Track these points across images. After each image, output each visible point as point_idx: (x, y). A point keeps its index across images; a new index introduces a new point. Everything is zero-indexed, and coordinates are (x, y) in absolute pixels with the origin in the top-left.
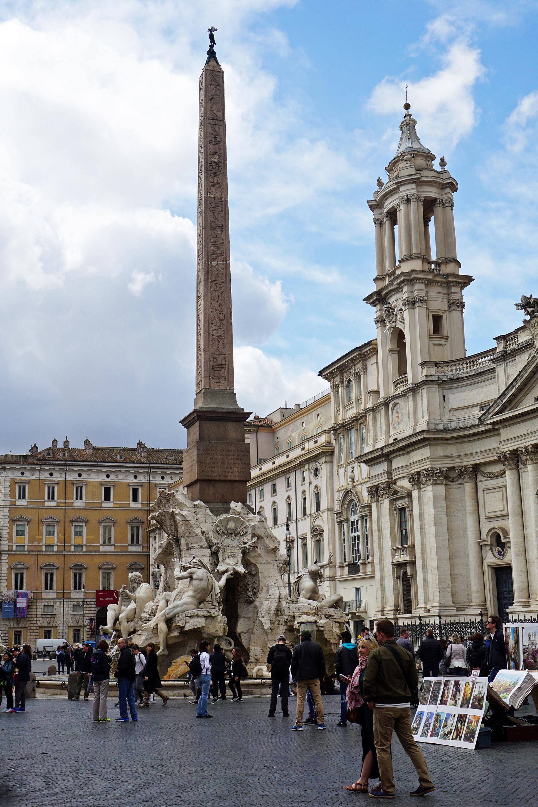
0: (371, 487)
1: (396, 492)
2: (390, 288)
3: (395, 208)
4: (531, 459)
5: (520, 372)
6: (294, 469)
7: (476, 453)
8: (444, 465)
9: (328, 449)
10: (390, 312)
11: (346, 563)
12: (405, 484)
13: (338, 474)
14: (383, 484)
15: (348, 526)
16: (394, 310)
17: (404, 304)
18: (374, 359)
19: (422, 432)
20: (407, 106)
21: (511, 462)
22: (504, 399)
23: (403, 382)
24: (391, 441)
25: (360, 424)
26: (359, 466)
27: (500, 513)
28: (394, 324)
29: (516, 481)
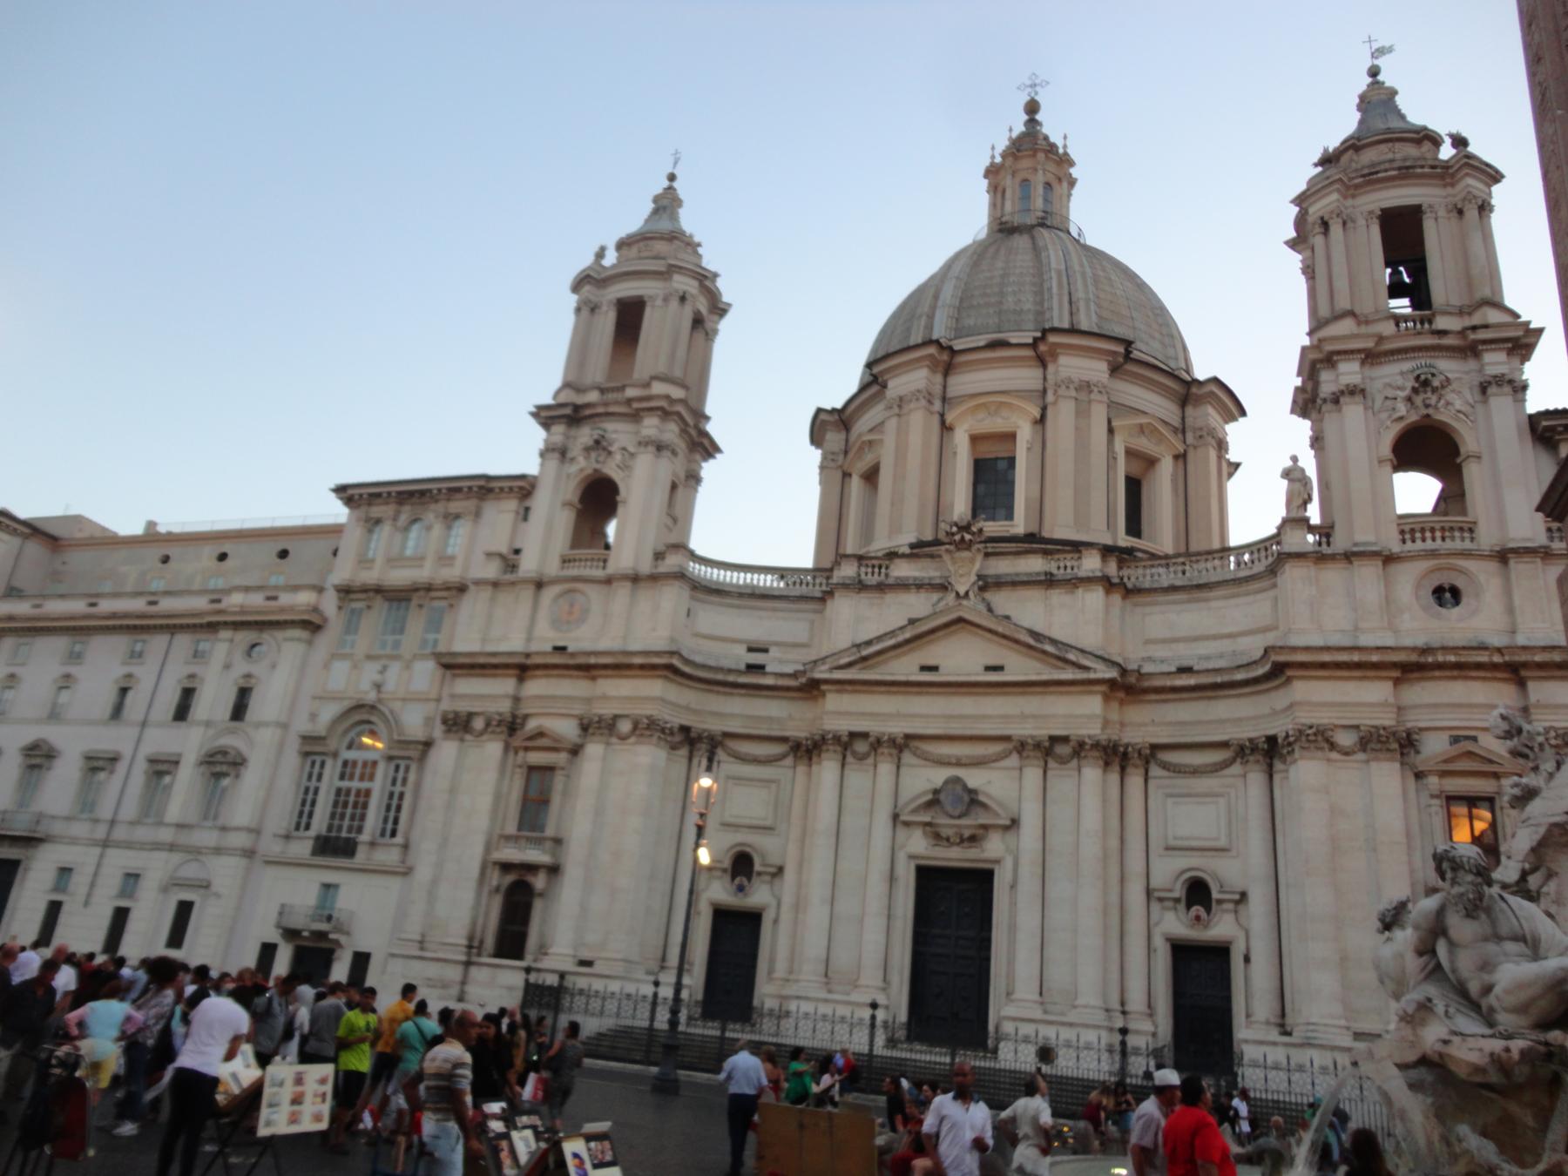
0: (456, 714)
1: (541, 734)
2: (612, 409)
3: (646, 299)
4: (891, 755)
5: (912, 622)
6: (173, 629)
7: (732, 715)
8: (676, 719)
9: (315, 619)
10: (599, 445)
11: (312, 832)
12: (567, 729)
13: (327, 666)
14: (500, 714)
15: (334, 766)
16: (610, 444)
17: (644, 443)
18: (511, 505)
19: (672, 653)
20: (672, 178)
21: (839, 749)
22: (865, 649)
23: (592, 560)
24: (548, 647)
25: (433, 599)
26: (408, 666)
27: (755, 822)
28: (598, 466)
29: (838, 782)
